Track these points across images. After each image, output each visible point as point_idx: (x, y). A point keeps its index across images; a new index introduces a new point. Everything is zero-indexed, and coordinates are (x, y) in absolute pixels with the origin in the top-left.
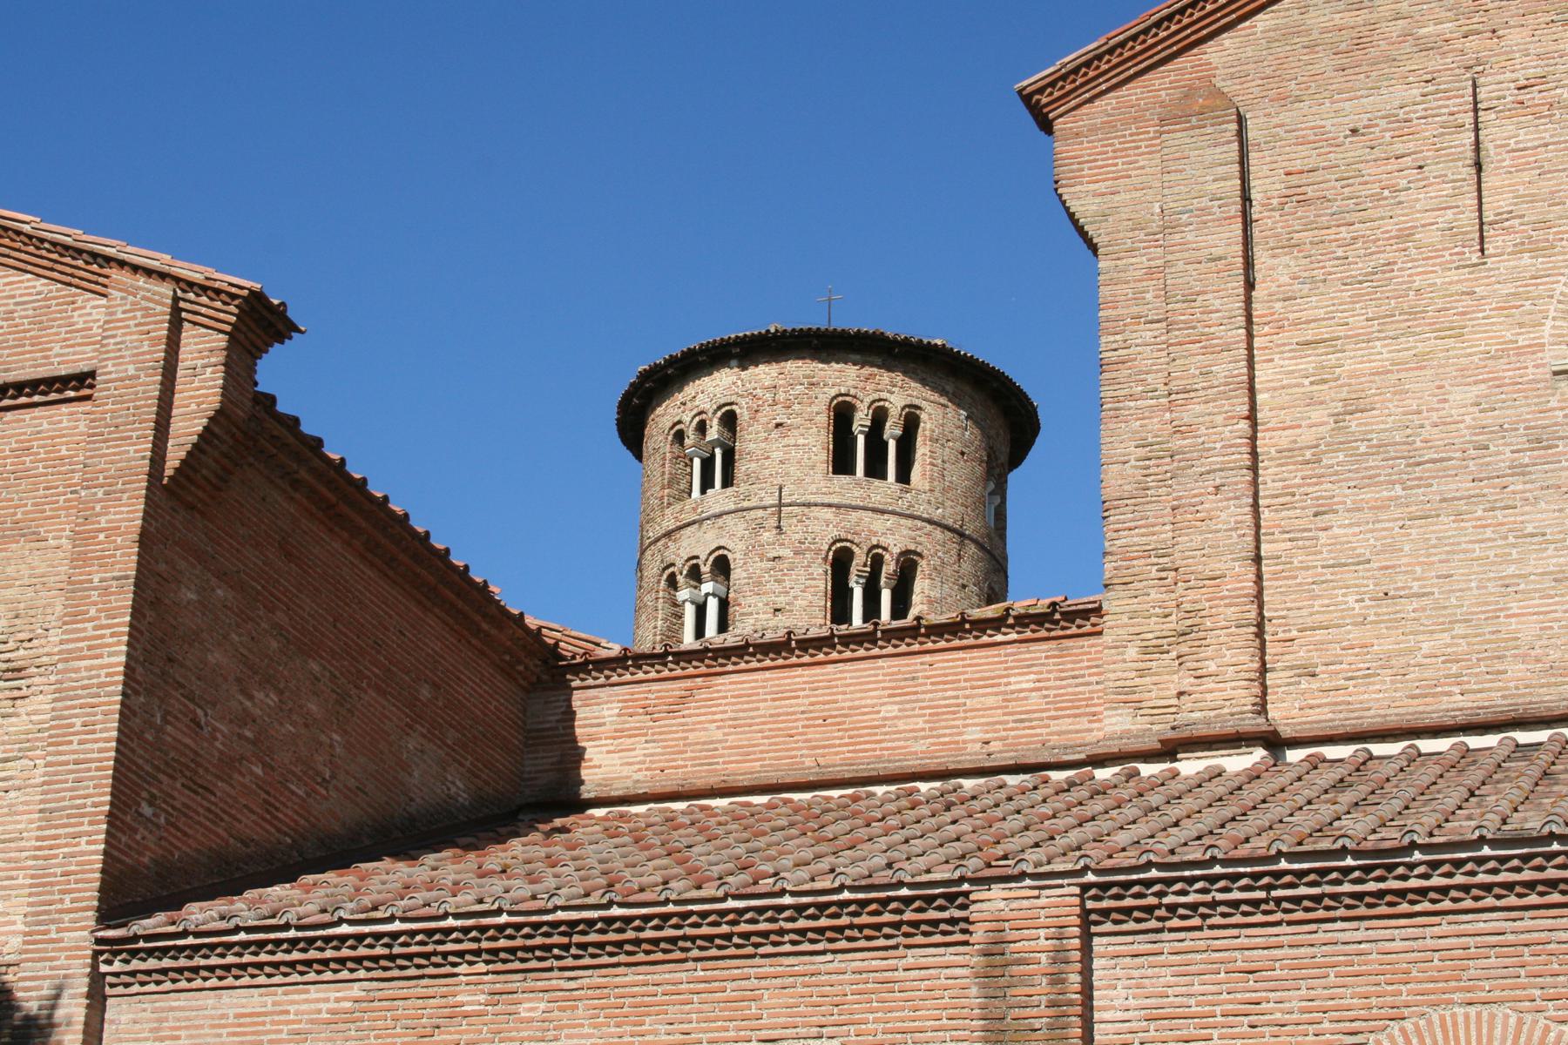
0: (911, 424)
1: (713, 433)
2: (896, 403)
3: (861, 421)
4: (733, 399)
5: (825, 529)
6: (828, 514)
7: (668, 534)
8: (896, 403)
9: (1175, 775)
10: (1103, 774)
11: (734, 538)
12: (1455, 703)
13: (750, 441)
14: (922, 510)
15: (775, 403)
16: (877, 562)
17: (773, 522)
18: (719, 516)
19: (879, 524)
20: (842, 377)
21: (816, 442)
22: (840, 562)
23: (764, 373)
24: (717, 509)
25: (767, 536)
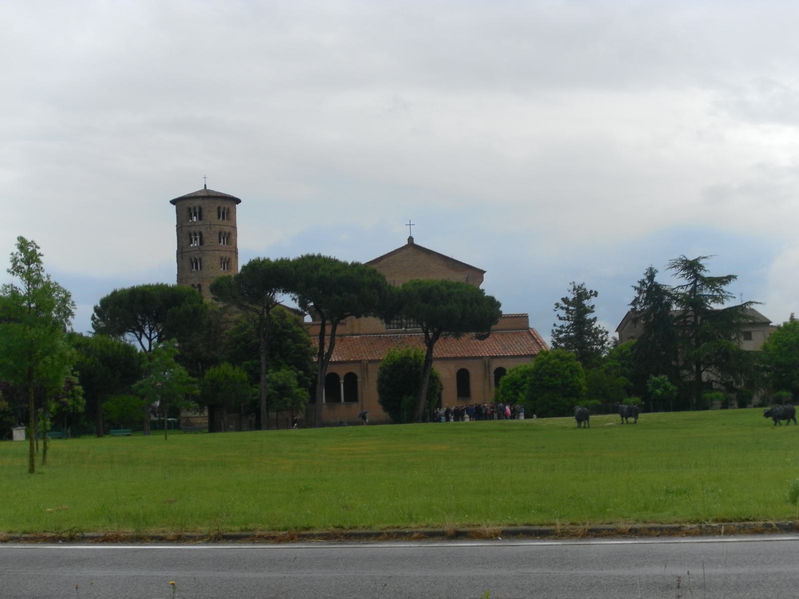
0: (228, 209)
1: (197, 210)
2: (227, 207)
3: (222, 210)
5: (217, 229)
6: (217, 226)
7: (189, 226)
8: (227, 207)
9: (353, 338)
10: (348, 336)
11: (203, 230)
12: (373, 332)
13: (205, 213)
14: (230, 225)
15: (209, 207)
16: (225, 233)
17: (209, 227)
18: (200, 225)
19: (225, 228)
20: (219, 203)
21: (215, 214)
22: (220, 233)
23: (206, 201)
25: (209, 230)
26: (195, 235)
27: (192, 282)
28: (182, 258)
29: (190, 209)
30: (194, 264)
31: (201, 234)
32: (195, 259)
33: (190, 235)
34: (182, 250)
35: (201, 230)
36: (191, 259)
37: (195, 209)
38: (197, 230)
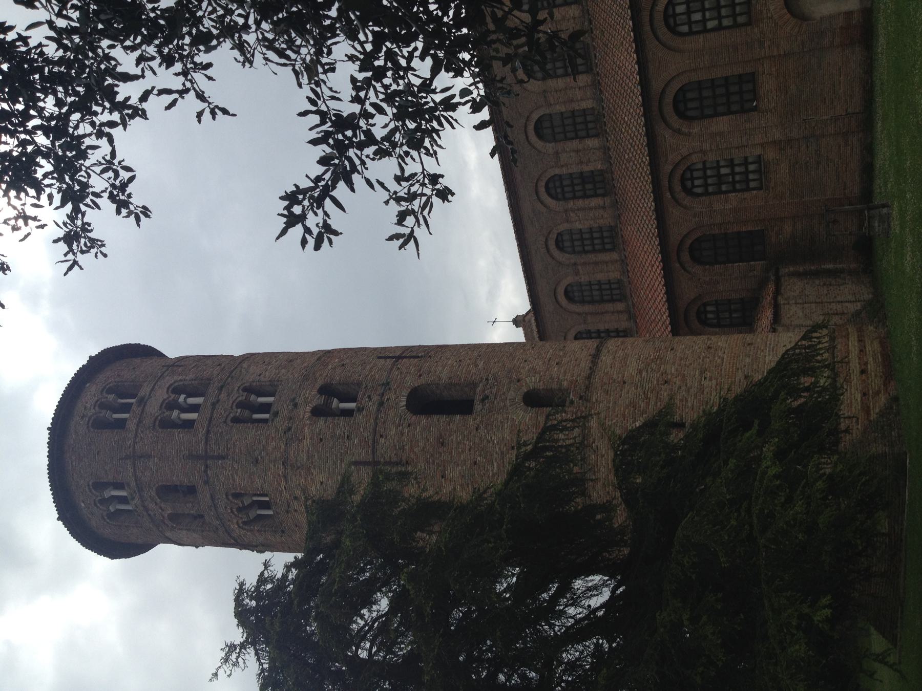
1: (111, 397)
4: (104, 385)
7: (140, 422)
11: (169, 380)
24: (149, 390)
25: (180, 369)
26: (171, 406)
27: (305, 411)
28: (222, 458)
29: (101, 424)
30: (256, 416)
31: (177, 391)
32: (240, 405)
33: (167, 424)
34: (198, 457)
35: (167, 386)
36: (236, 420)
37: (103, 406)
38: (161, 394)
